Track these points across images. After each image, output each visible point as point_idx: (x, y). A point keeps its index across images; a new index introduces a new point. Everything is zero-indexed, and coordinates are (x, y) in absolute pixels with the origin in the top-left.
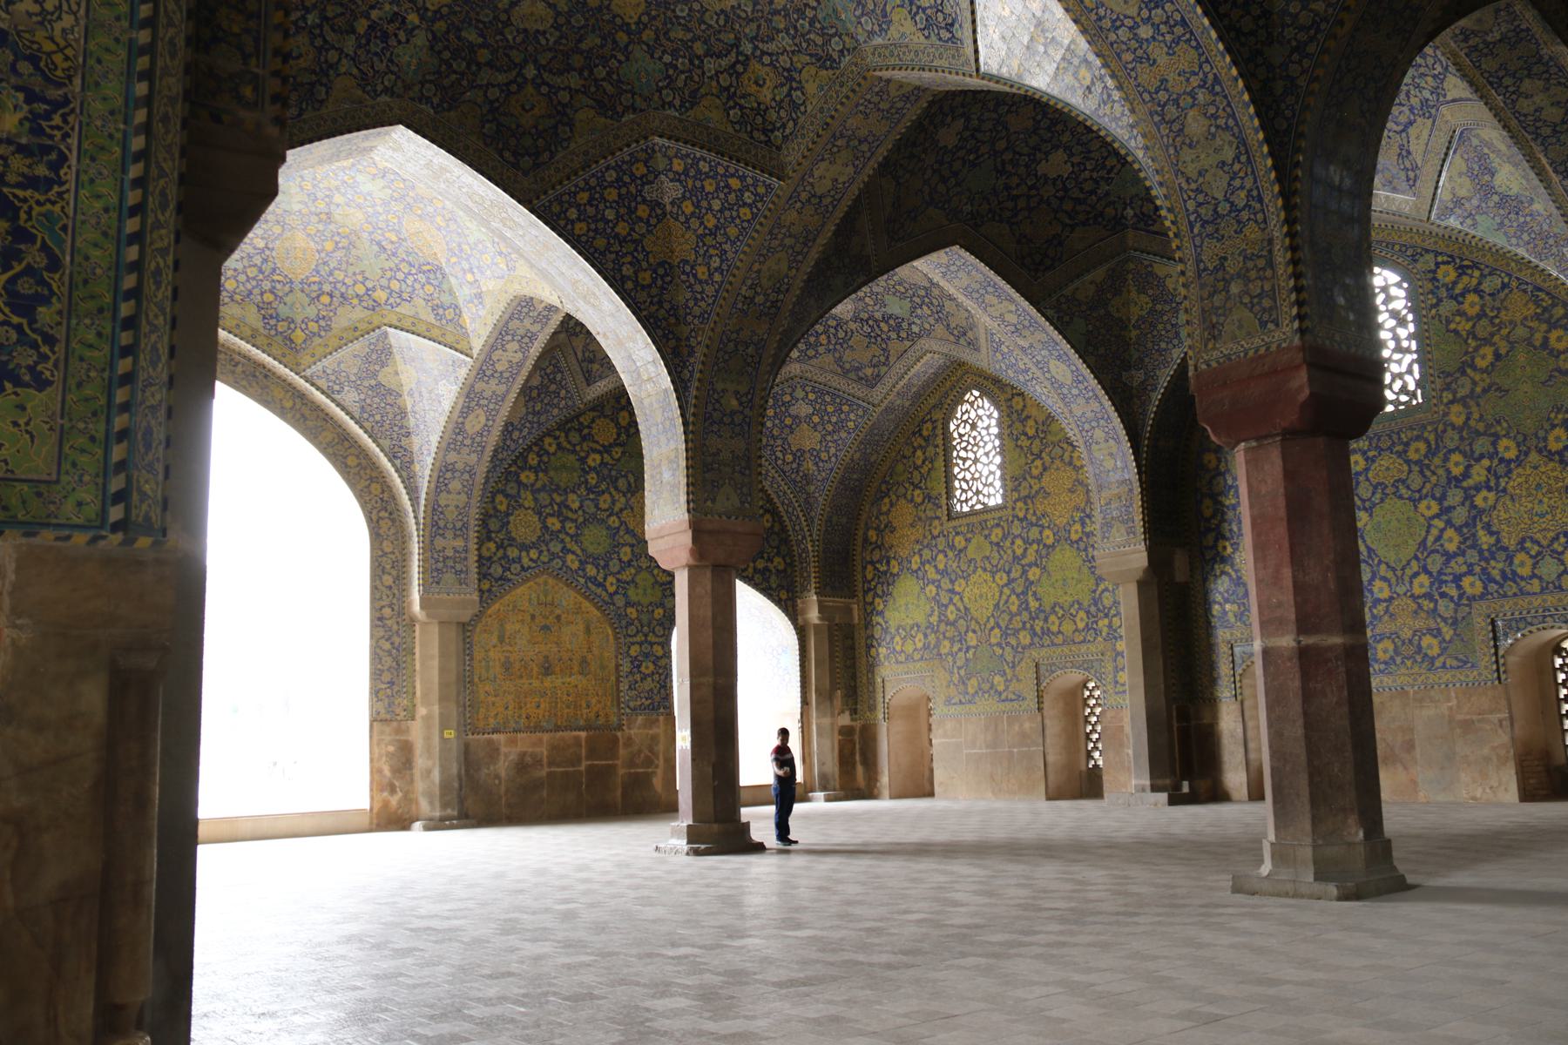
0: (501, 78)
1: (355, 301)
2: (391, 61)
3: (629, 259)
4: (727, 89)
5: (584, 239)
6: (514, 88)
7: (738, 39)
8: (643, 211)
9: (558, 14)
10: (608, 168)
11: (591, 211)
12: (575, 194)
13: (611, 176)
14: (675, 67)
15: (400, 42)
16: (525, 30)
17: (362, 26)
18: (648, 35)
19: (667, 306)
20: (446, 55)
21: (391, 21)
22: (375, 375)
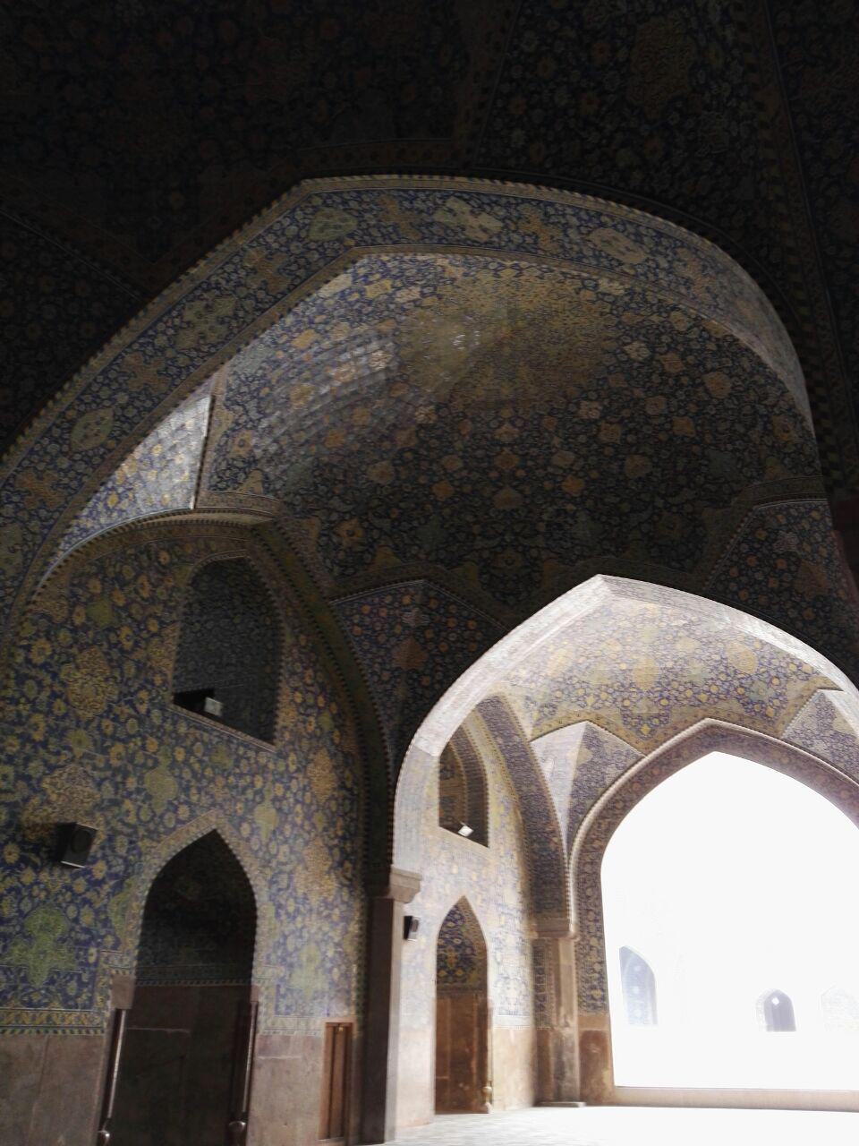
0: (645, 516)
1: (794, 677)
2: (573, 538)
3: (789, 605)
4: (773, 446)
5: (750, 602)
6: (656, 518)
7: (753, 407)
8: (782, 564)
9: (651, 457)
10: (739, 543)
11: (744, 579)
12: (728, 571)
13: (745, 548)
14: (738, 450)
15: (571, 525)
16: (640, 478)
17: (542, 527)
18: (708, 438)
19: (835, 631)
20: (604, 519)
21: (558, 515)
22: (830, 727)
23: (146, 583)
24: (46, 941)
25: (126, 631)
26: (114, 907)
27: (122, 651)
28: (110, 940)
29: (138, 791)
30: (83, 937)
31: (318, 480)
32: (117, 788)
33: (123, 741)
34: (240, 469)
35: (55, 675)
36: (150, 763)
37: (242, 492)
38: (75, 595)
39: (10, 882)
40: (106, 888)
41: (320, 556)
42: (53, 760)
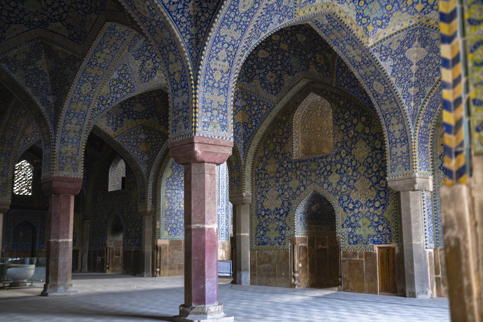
23: (281, 131)
24: (273, 231)
25: (278, 147)
26: (287, 220)
27: (278, 154)
28: (287, 228)
29: (288, 188)
30: (281, 228)
31: (299, 57)
32: (282, 189)
33: (282, 177)
34: (279, 81)
35: (264, 170)
36: (290, 179)
37: (286, 84)
38: (265, 147)
39: (264, 219)
40: (284, 215)
41: (321, 74)
42: (267, 190)
